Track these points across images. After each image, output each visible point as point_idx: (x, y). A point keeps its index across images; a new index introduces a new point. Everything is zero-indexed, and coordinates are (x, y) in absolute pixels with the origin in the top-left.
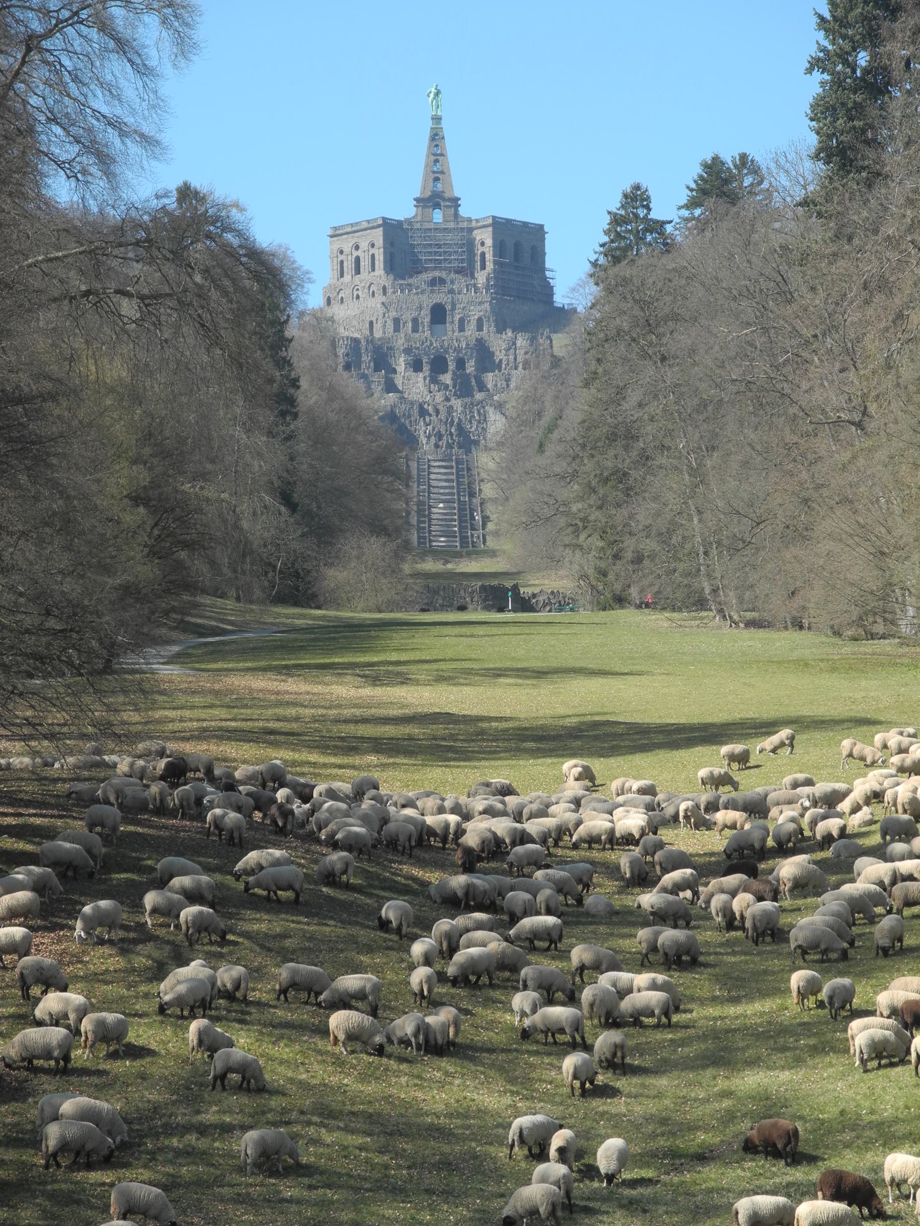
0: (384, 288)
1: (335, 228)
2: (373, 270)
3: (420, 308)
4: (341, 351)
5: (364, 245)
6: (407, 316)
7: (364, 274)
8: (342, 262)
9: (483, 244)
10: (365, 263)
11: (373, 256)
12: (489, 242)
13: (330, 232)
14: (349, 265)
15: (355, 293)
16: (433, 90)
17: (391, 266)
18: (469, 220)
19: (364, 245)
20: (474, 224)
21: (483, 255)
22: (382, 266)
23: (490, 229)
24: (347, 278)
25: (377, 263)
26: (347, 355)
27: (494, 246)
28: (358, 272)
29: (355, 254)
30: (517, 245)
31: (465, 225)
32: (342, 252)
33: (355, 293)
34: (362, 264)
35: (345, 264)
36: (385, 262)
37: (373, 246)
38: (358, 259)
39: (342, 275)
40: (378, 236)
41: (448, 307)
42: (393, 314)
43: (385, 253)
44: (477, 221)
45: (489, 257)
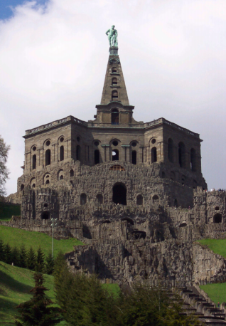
1: (30, 131)
2: (62, 158)
7: (54, 164)
8: (35, 156)
10: (55, 155)
11: (62, 148)
12: (160, 138)
13: (24, 134)
14: (41, 157)
16: (111, 30)
18: (141, 123)
20: (146, 126)
21: (154, 150)
22: (70, 154)
23: (161, 128)
24: (39, 168)
27: (164, 142)
28: (48, 162)
32: (35, 149)
33: (46, 179)
35: (37, 157)
38: (48, 152)
39: (34, 167)
41: (128, 187)
42: (81, 191)
43: (72, 144)
44: (148, 123)
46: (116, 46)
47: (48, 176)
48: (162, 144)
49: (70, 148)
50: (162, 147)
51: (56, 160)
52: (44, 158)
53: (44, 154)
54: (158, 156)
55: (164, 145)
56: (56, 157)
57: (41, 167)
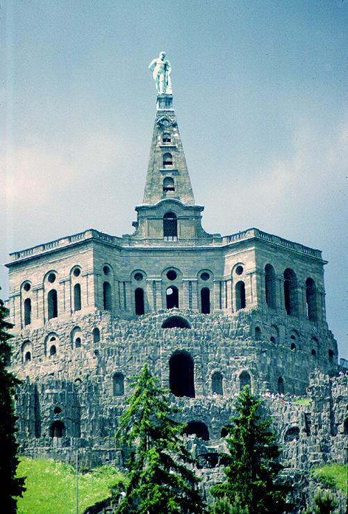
0: (96, 332)
2: (78, 306)
3: (153, 359)
4: (46, 406)
5: (63, 271)
6: (136, 368)
8: (28, 302)
9: (240, 270)
11: (78, 287)
12: (250, 265)
15: (50, 344)
17: (105, 300)
19: (63, 271)
20: (225, 243)
21: (241, 286)
22: (92, 300)
25: (83, 296)
26: (57, 410)
29: (49, 287)
30: (289, 273)
31: (214, 245)
32: (27, 287)
33: (50, 344)
34: (60, 300)
35: (33, 304)
36: (96, 295)
37: (77, 272)
38: (53, 294)
40: (86, 259)
41: (197, 359)
42: (113, 368)
43: (96, 282)
45: (251, 287)
46: (169, 91)
47: (53, 339)
48: (254, 276)
49: (91, 289)
50: (255, 282)
51: (68, 309)
52: (46, 305)
53: (46, 297)
54: (248, 298)
55: (257, 279)
56: (68, 304)
57: (40, 321)
